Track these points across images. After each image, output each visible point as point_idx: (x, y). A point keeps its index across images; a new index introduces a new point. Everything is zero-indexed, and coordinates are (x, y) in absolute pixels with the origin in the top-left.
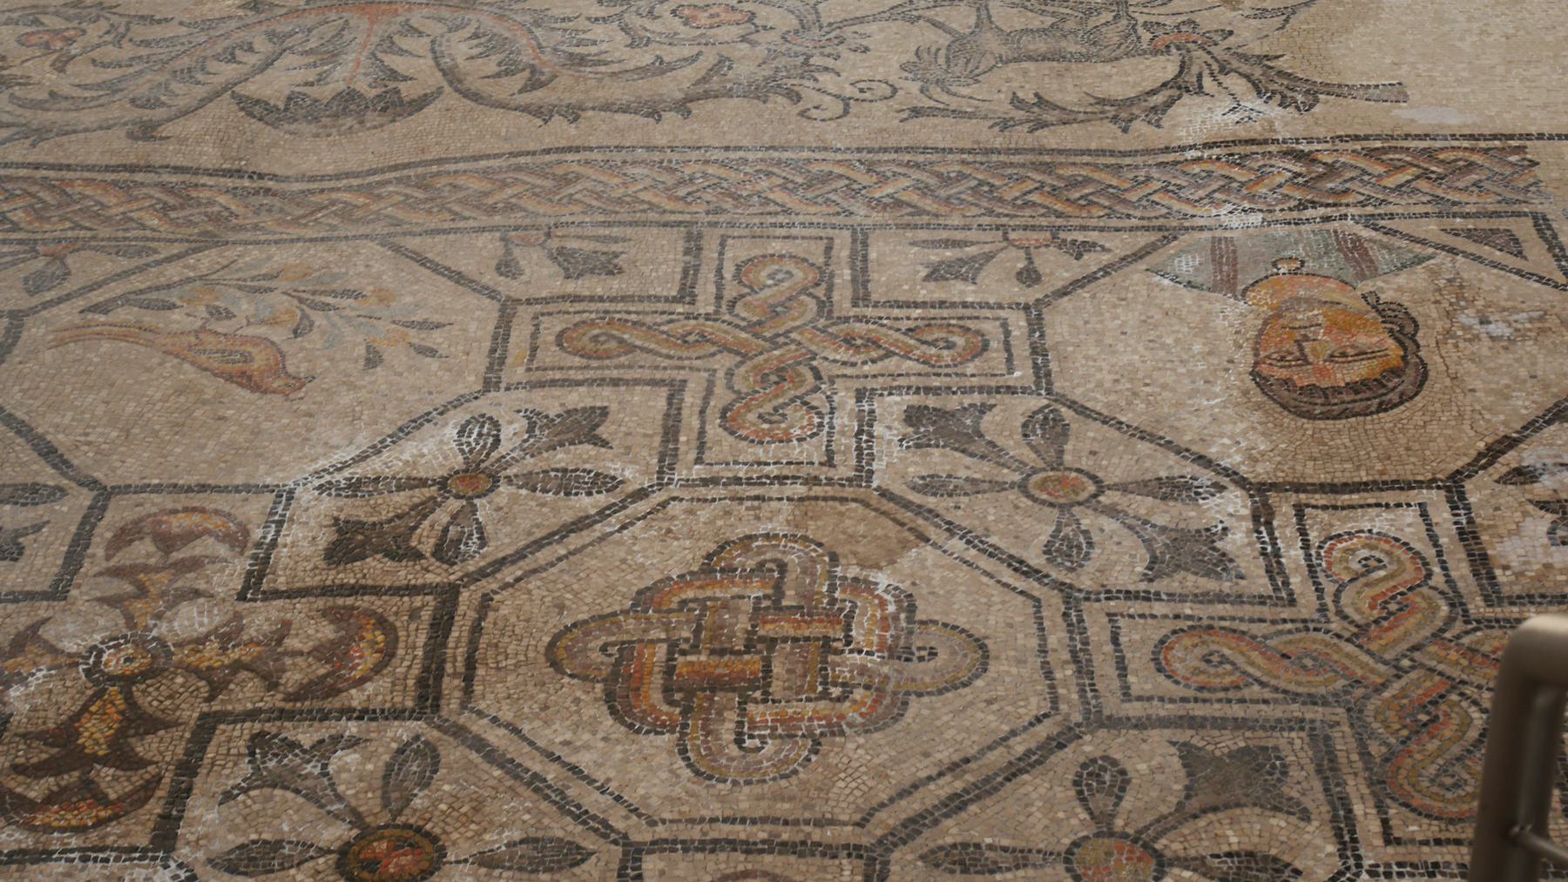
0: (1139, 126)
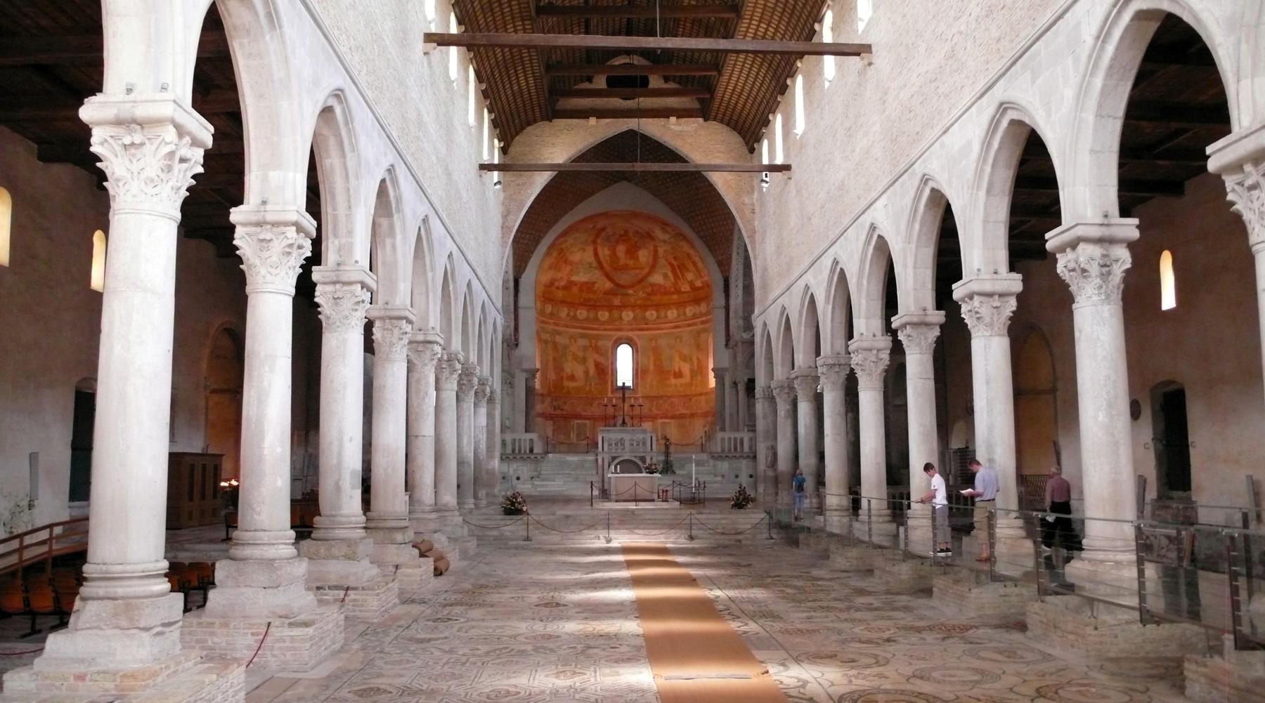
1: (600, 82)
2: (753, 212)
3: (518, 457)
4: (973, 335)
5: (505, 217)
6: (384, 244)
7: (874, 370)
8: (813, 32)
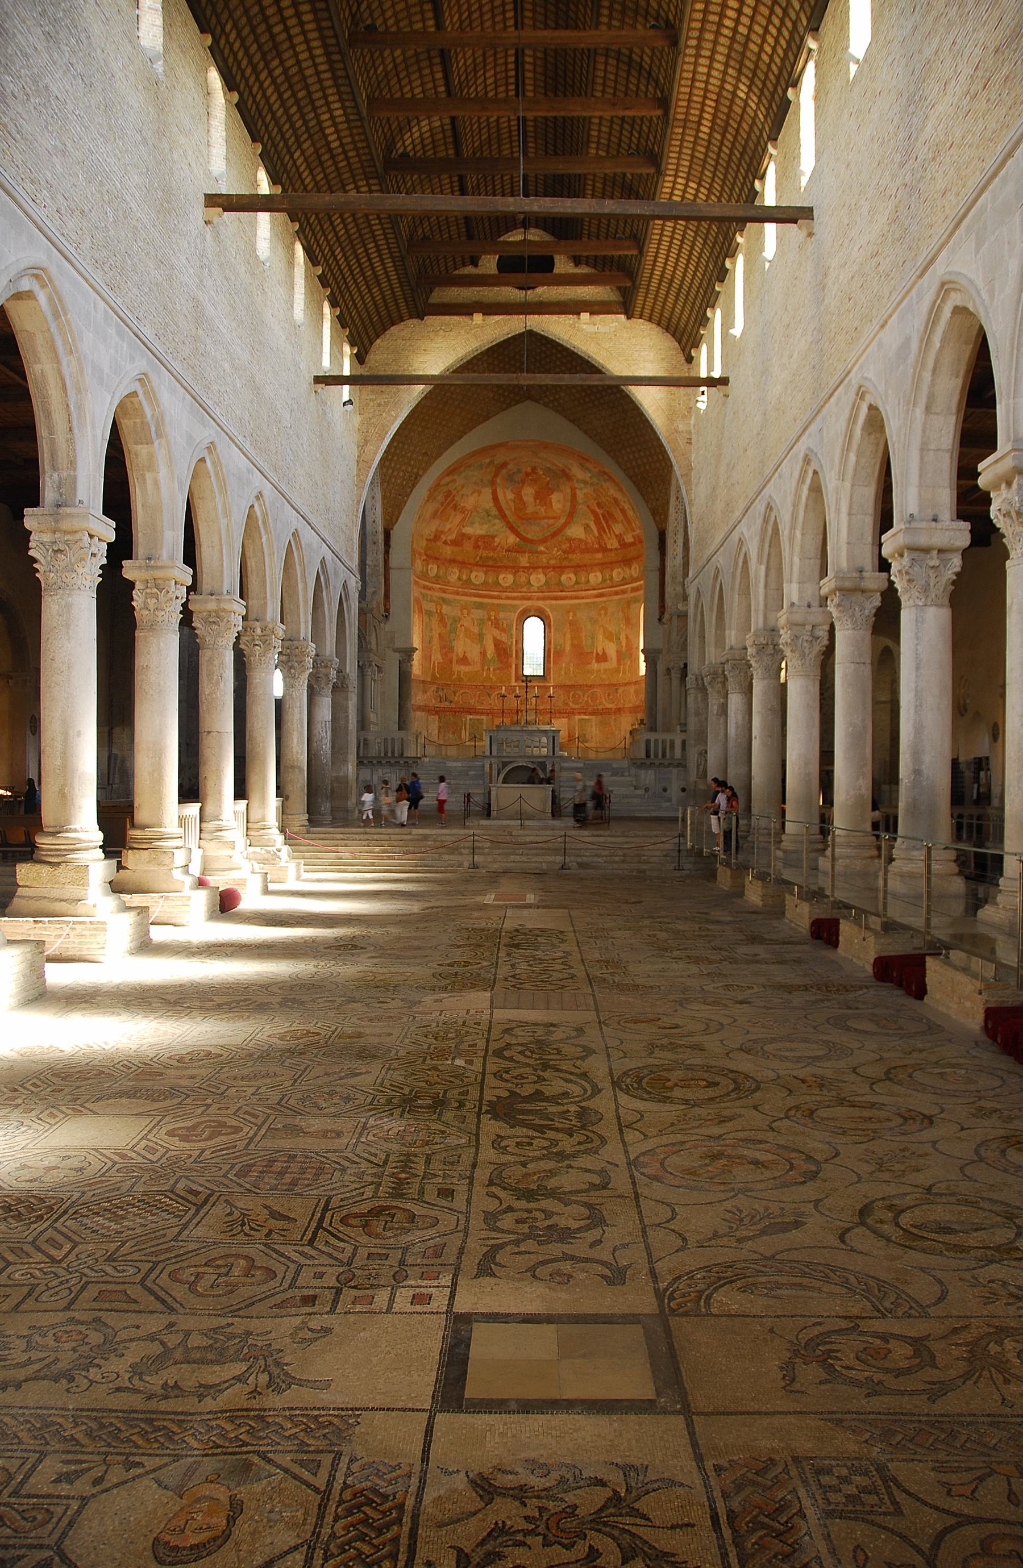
0: (208, 1399)
1: (489, 264)
2: (689, 442)
3: (384, 762)
4: (903, 603)
5: (362, 446)
6: (144, 481)
7: (807, 651)
8: (754, 194)
